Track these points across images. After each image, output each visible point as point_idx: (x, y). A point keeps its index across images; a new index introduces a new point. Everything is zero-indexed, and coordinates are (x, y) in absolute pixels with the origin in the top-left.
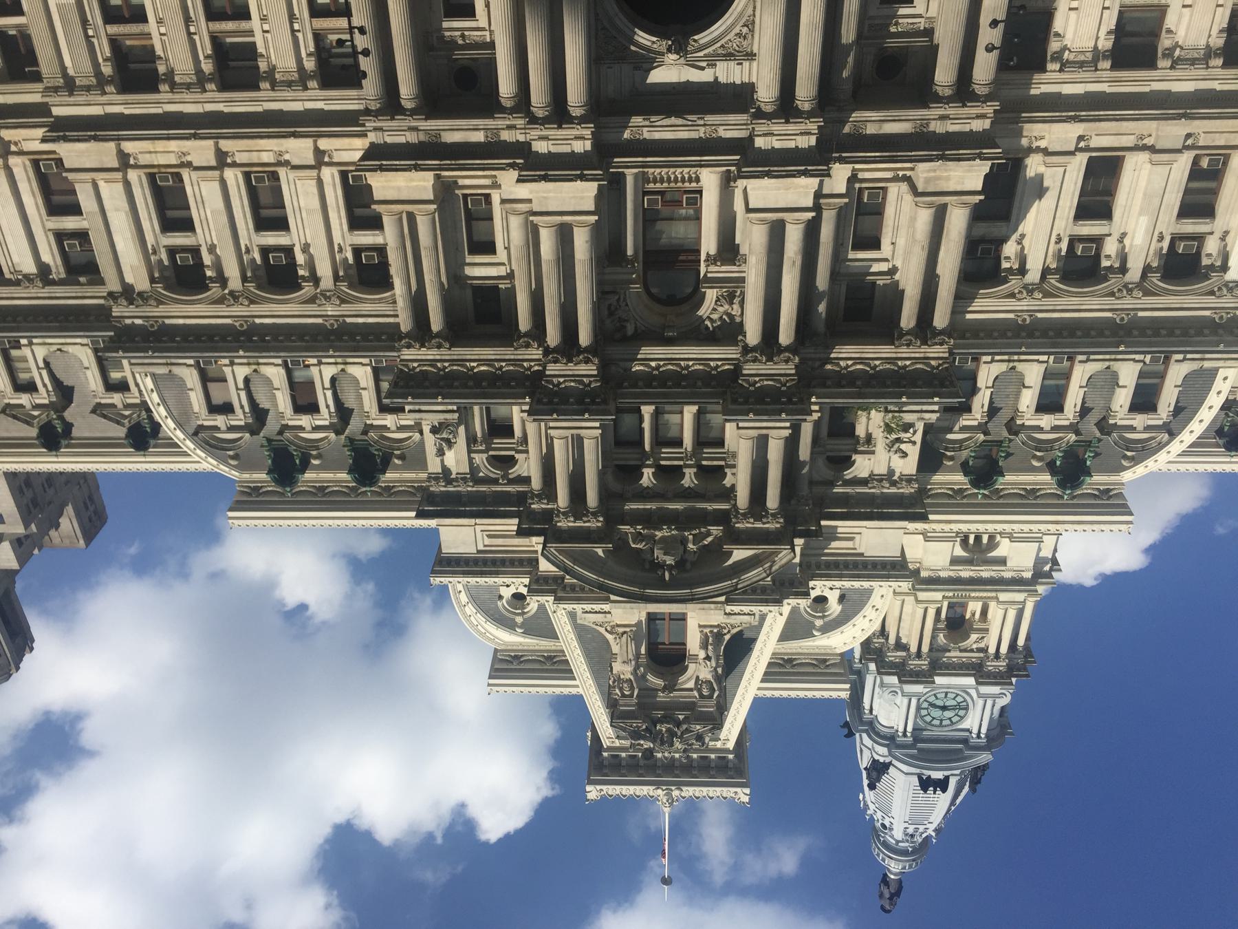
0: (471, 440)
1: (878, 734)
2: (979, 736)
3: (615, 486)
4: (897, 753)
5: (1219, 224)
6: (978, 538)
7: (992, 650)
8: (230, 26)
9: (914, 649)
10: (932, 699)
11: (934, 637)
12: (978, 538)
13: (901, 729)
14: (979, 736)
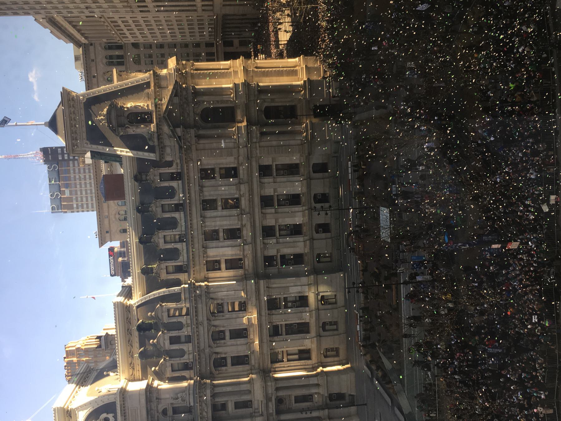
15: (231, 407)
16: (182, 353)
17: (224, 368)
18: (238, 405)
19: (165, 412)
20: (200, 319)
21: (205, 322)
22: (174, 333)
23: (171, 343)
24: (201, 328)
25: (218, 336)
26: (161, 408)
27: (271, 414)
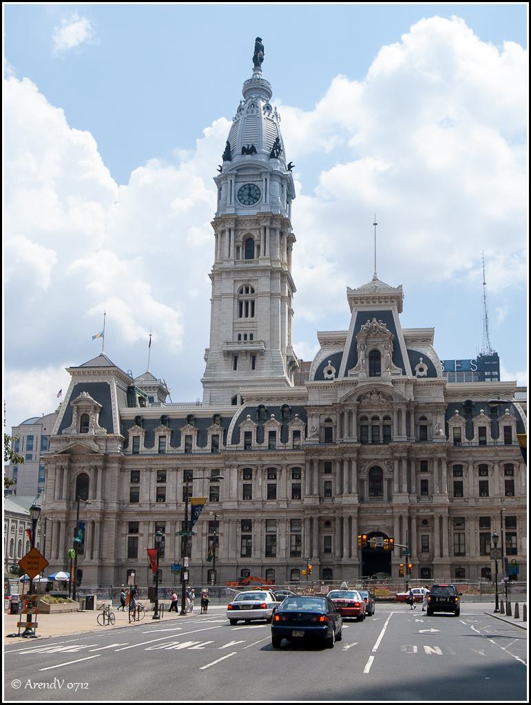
0: (431, 424)
1: (279, 176)
2: (231, 181)
3: (390, 415)
4: (270, 170)
5: (241, 485)
6: (247, 292)
7: (232, 233)
8: (485, 531)
9: (268, 231)
10: (255, 201)
11: (260, 236)
12: (247, 292)
13: (268, 182)
14: (231, 181)
15: (424, 476)
16: (470, 436)
17: (452, 474)
18: (424, 482)
19: (424, 418)
20: (500, 454)
21: (497, 458)
22: (488, 431)
23: (480, 428)
24: (492, 454)
25: (483, 469)
26: (429, 416)
27: (418, 511)
